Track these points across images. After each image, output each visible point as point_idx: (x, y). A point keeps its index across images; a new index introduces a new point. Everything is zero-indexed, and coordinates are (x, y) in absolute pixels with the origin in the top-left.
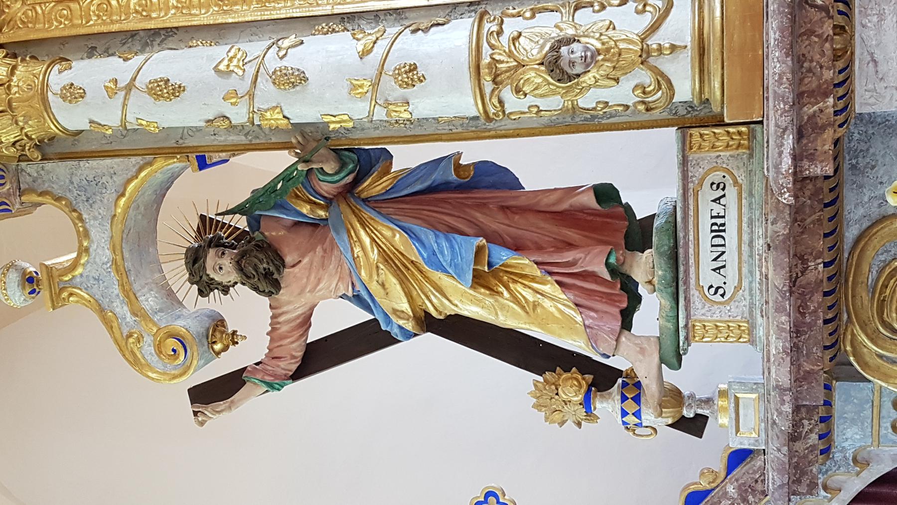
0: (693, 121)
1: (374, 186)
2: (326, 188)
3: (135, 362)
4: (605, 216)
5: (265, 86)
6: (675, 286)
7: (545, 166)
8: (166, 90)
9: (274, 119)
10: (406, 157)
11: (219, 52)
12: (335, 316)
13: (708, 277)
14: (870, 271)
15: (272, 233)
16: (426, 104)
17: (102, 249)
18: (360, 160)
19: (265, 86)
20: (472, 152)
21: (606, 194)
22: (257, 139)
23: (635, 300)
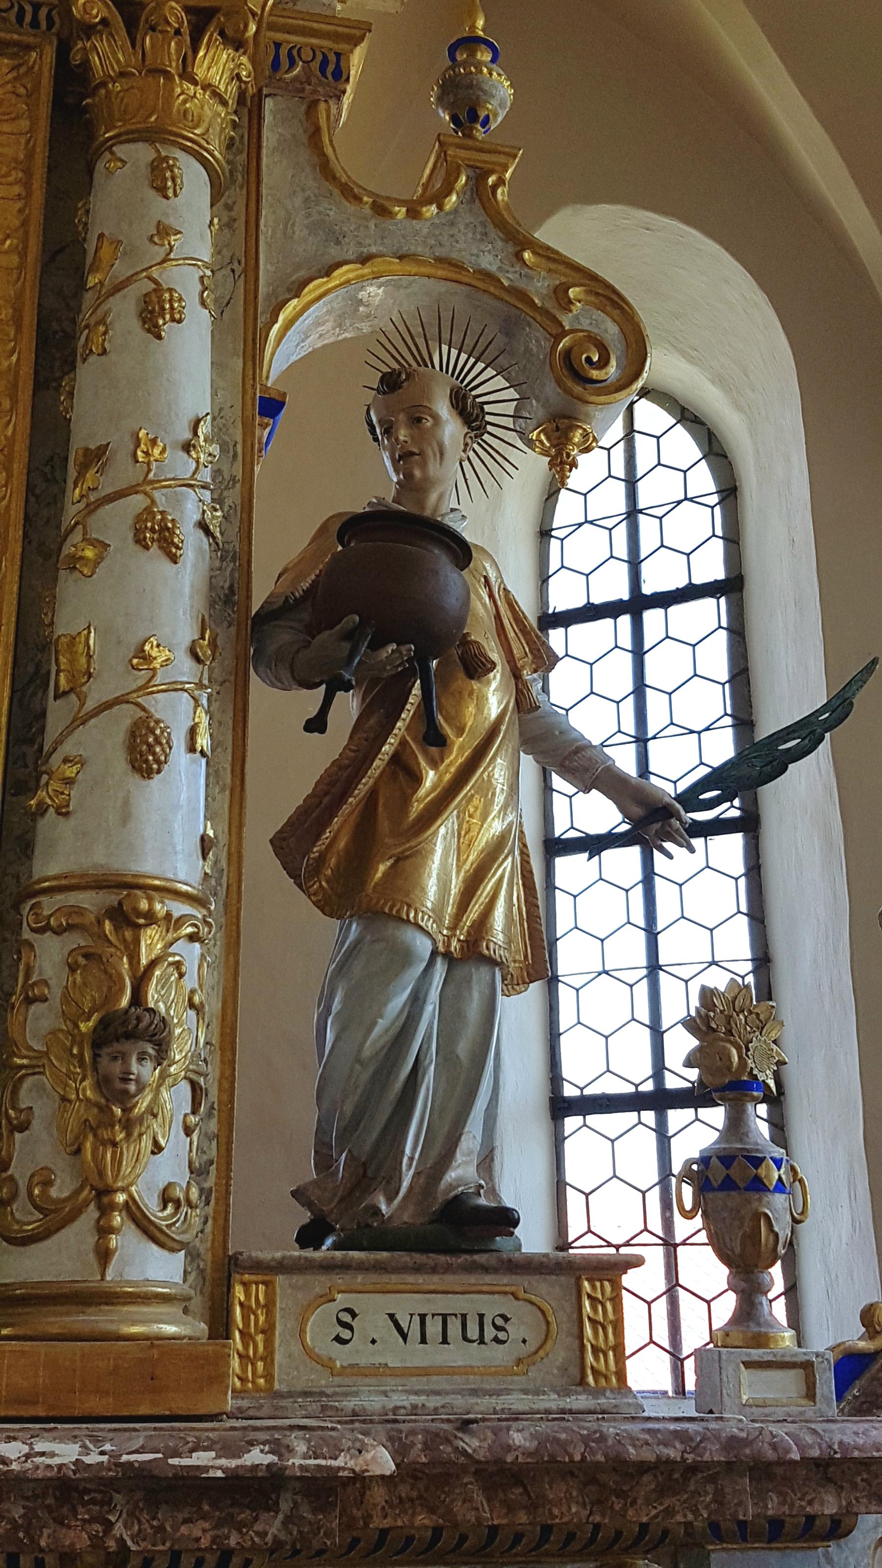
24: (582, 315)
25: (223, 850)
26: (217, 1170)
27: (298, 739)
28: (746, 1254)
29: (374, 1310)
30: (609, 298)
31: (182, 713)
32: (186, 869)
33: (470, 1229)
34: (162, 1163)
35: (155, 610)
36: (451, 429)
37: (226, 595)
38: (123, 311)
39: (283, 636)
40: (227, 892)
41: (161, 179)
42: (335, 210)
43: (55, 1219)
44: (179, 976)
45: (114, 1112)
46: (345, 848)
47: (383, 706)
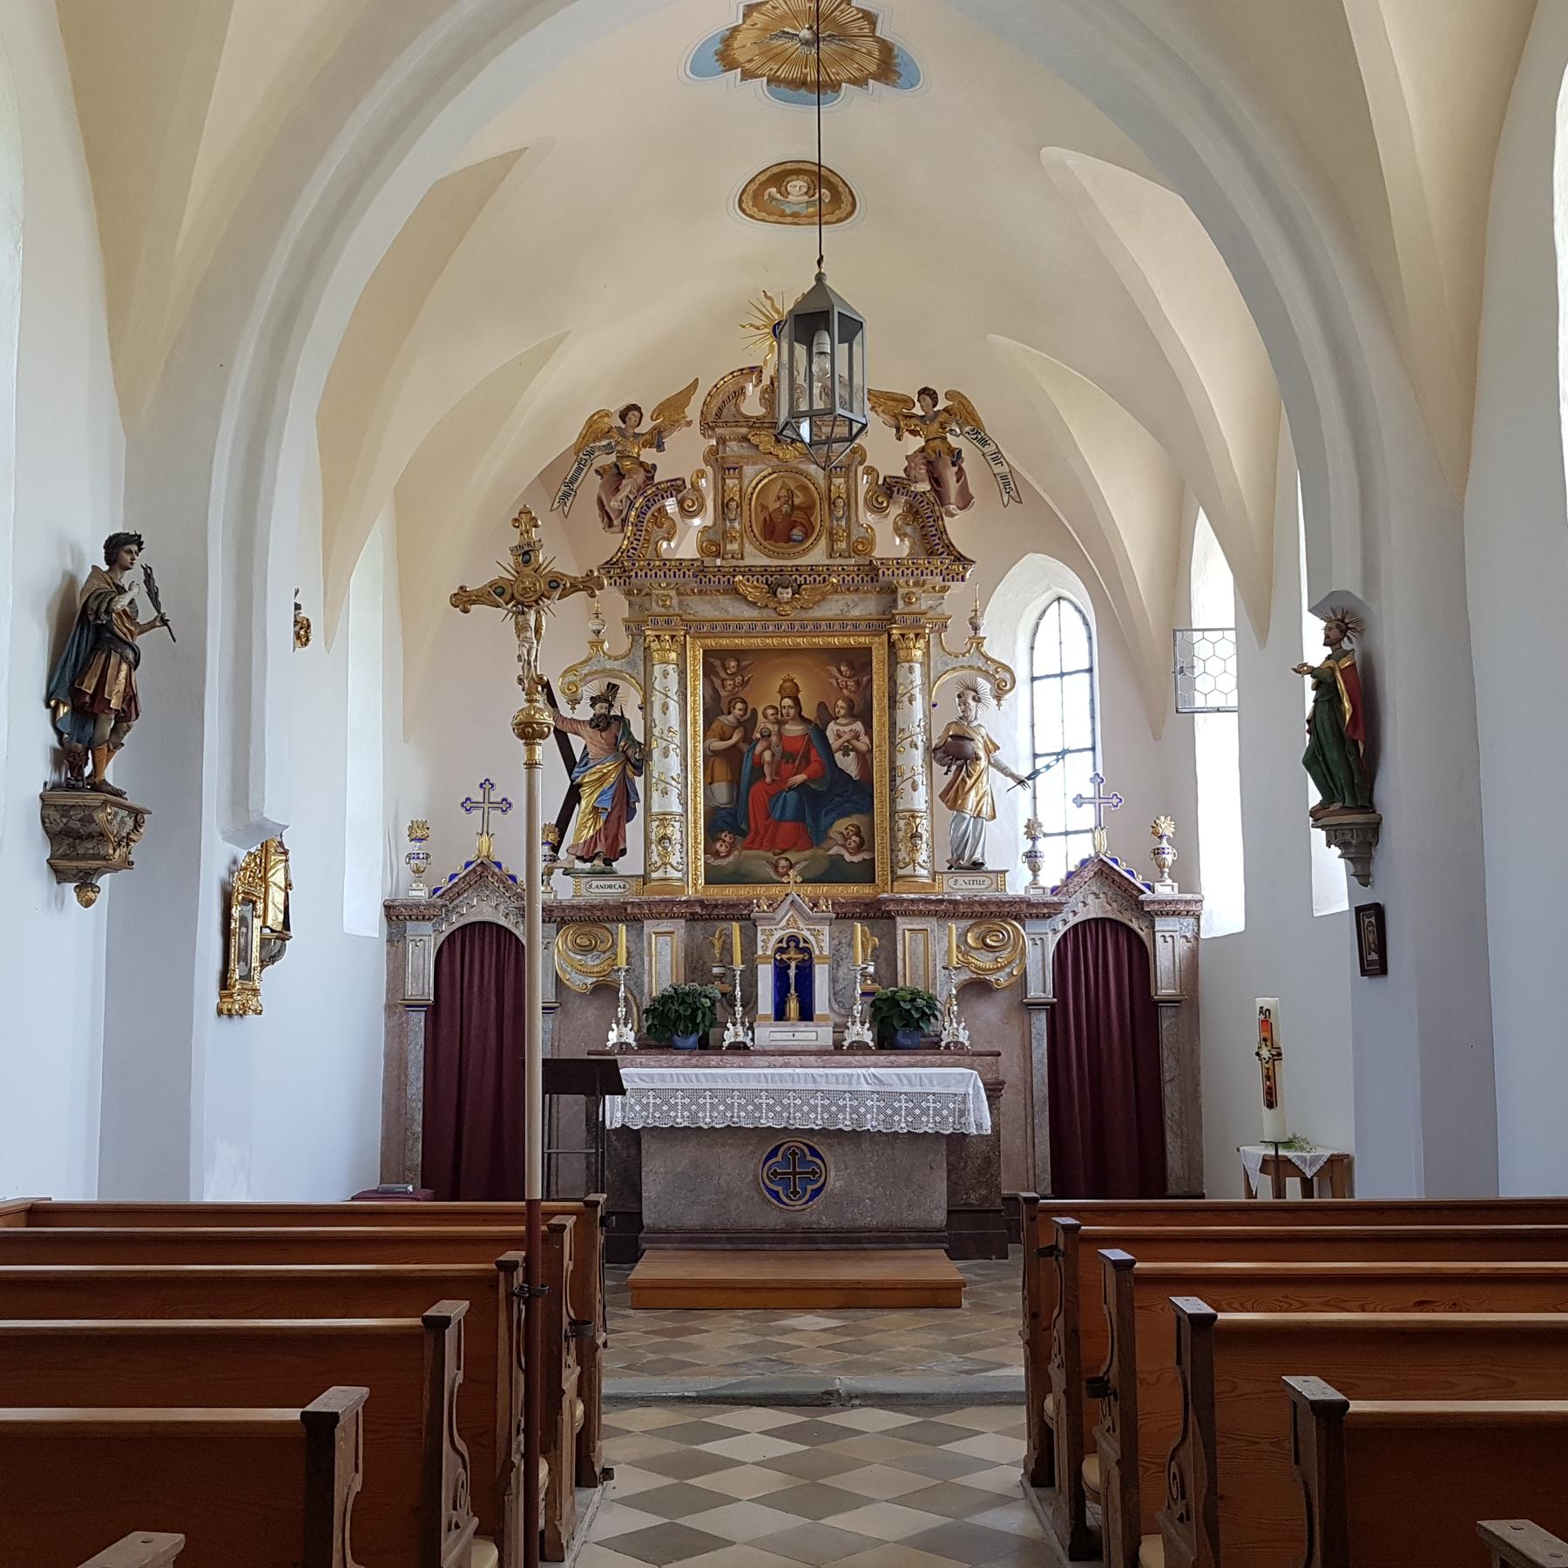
0: (645, 878)
1: (629, 768)
2: (630, 752)
3: (566, 672)
4: (616, 850)
5: (665, 744)
6: (593, 873)
7: (633, 831)
8: (665, 708)
9: (654, 745)
10: (639, 782)
11: (676, 728)
12: (577, 744)
13: (595, 884)
14: (595, 930)
15: (614, 727)
16: (655, 795)
17: (609, 665)
18: (640, 766)
19: (665, 744)
20: (639, 807)
21: (623, 852)
22: (648, 731)
23: (585, 861)
24: (1002, 674)
25: (930, 802)
26: (932, 857)
27: (943, 777)
28: (1035, 870)
29: (961, 880)
30: (1007, 669)
31: (921, 779)
32: (923, 806)
33: (977, 866)
34: (923, 856)
35: (914, 760)
36: (973, 704)
37: (927, 748)
38: (905, 699)
39: (940, 755)
40: (931, 808)
41: (911, 670)
42: (948, 658)
43: (907, 865)
44: (923, 826)
45: (914, 849)
46: (953, 797)
47: (960, 769)
